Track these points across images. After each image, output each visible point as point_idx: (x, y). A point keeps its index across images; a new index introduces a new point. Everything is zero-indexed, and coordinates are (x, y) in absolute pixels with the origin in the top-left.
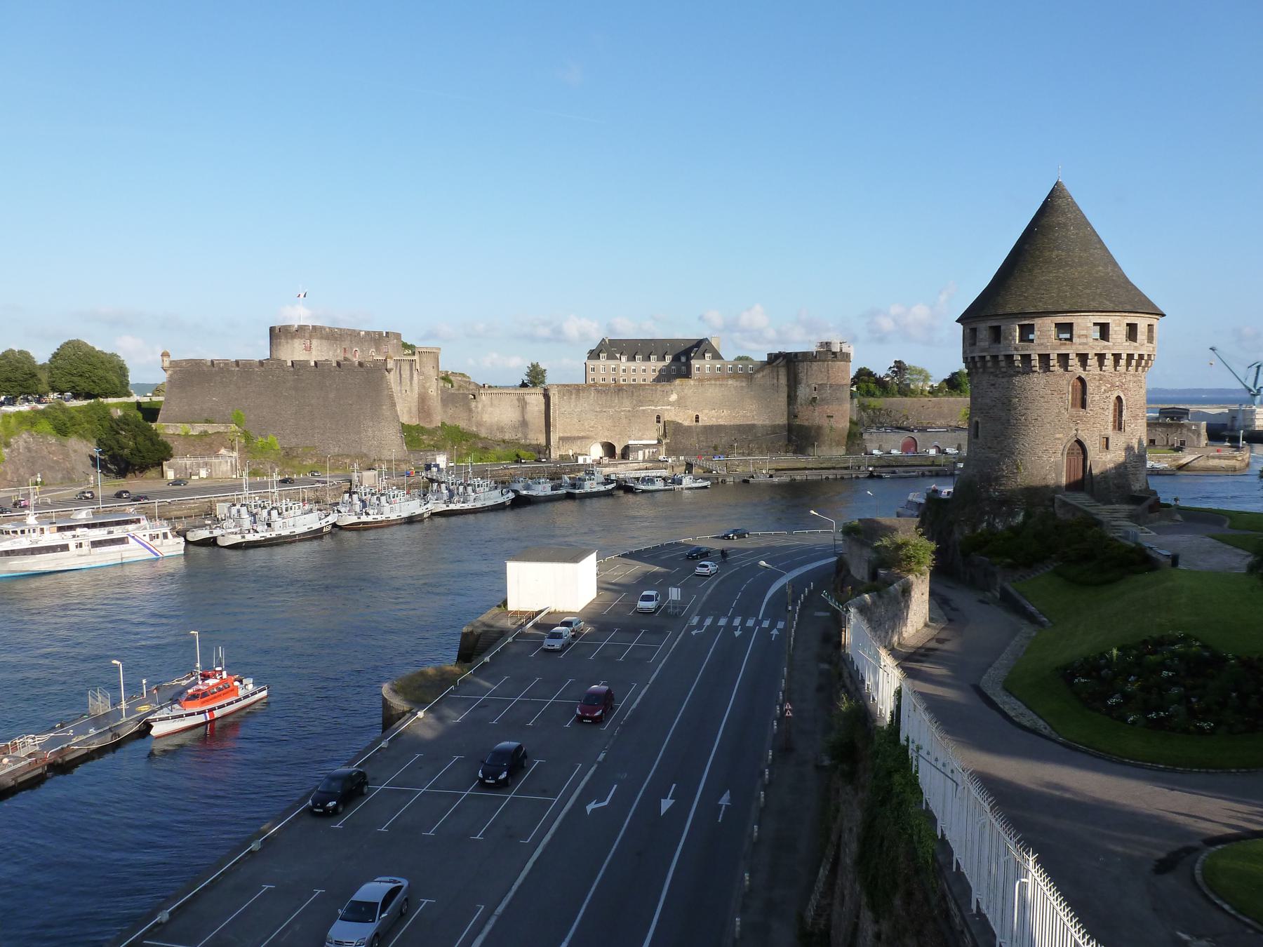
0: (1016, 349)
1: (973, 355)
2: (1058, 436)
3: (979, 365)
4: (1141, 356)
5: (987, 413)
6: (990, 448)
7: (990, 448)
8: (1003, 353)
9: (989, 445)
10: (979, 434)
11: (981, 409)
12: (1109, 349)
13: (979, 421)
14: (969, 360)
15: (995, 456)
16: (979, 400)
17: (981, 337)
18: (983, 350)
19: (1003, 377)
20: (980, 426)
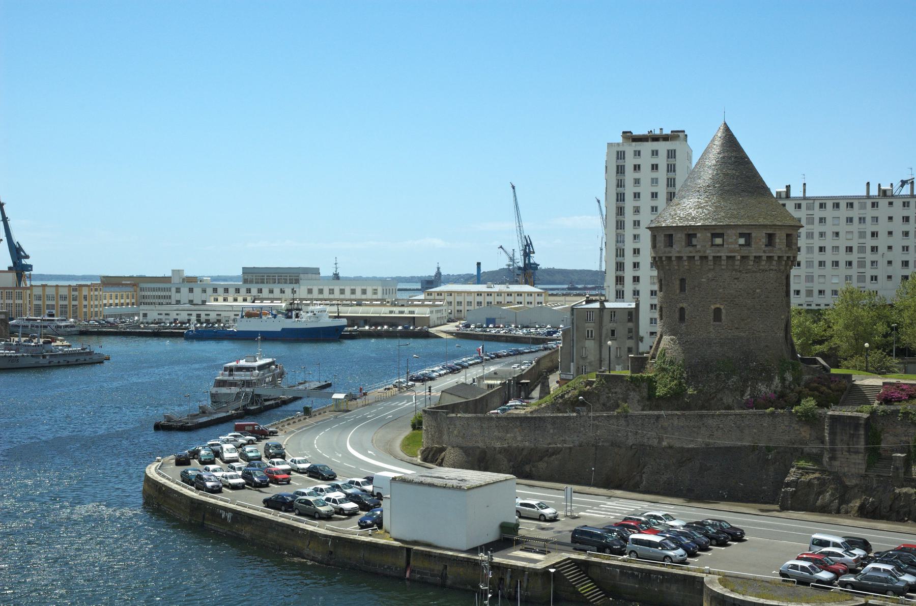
0: (764, 252)
1: (719, 255)
2: (783, 317)
3: (724, 263)
4: (788, 258)
5: (732, 301)
6: (737, 328)
7: (737, 328)
8: (754, 254)
9: (736, 326)
10: (723, 317)
11: (721, 298)
12: (753, 252)
13: (722, 307)
14: (657, 259)
15: (742, 334)
16: (720, 290)
17: (730, 240)
18: (731, 251)
19: (746, 273)
20: (724, 311)
